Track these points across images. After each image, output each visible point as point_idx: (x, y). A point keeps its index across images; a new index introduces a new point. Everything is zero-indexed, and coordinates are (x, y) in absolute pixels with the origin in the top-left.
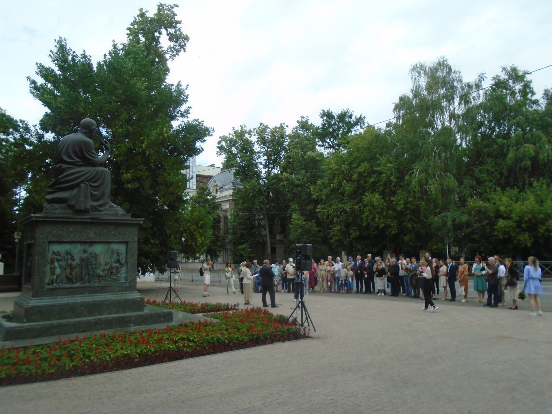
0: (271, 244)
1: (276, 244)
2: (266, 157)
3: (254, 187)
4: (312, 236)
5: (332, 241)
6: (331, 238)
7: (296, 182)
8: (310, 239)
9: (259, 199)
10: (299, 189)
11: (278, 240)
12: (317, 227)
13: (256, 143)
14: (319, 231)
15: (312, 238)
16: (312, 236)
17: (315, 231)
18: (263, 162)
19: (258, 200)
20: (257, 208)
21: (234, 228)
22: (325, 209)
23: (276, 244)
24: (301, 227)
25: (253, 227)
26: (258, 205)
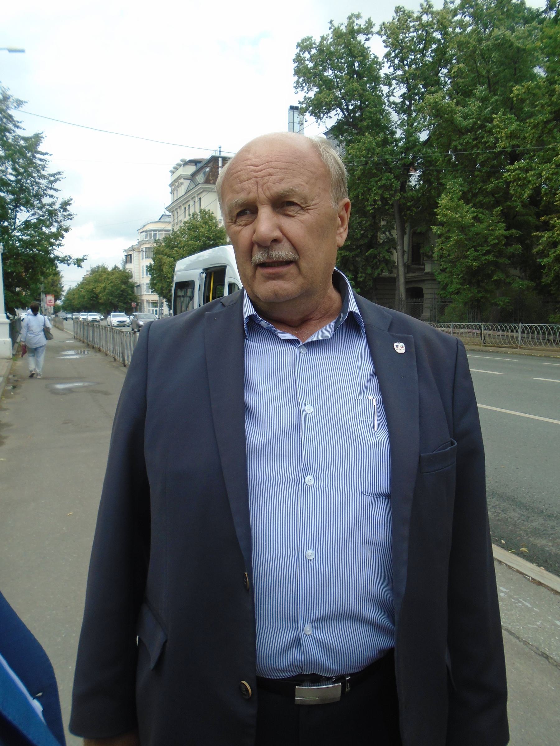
0: (407, 282)
1: (424, 281)
2: (403, 89)
3: (368, 150)
4: (488, 252)
5: (544, 261)
6: (543, 254)
7: (458, 118)
8: (484, 258)
9: (380, 180)
10: (468, 137)
11: (427, 274)
12: (508, 228)
13: (386, 60)
14: (509, 240)
15: (490, 257)
16: (488, 252)
17: (497, 238)
18: (398, 100)
19: (377, 182)
20: (375, 201)
21: (247, 218)
22: (531, 169)
23: (424, 281)
24: (463, 228)
25: (372, 243)
26: (376, 194)
